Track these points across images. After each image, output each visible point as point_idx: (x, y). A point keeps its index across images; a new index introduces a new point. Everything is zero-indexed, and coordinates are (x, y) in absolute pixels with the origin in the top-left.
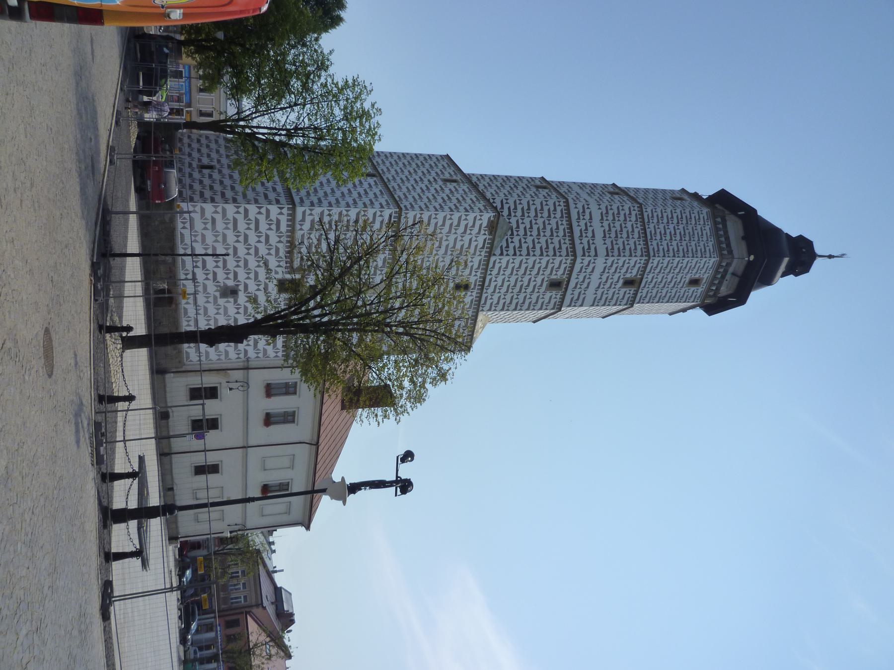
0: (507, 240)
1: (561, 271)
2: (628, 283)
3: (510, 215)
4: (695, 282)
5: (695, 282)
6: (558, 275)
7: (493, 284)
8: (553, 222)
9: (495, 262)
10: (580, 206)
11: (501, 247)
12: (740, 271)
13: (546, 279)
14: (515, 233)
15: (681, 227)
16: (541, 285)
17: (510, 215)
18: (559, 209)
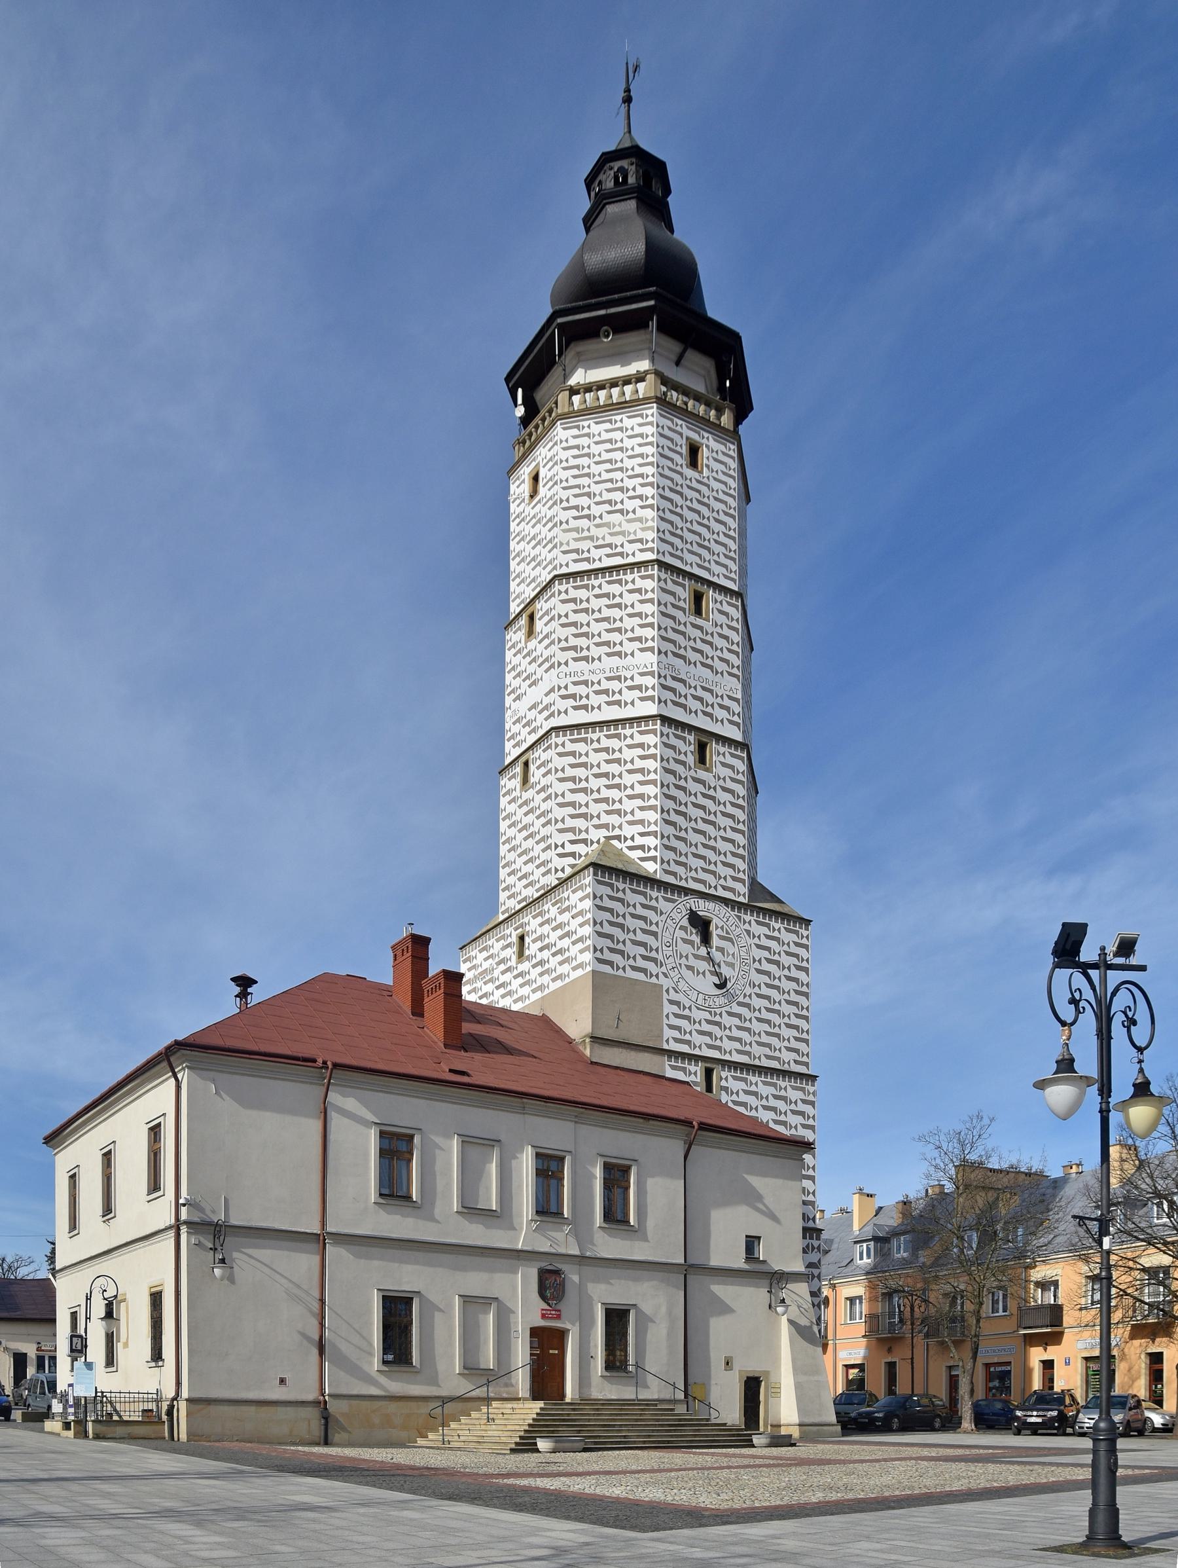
0: (630, 848)
1: (679, 744)
3: (585, 841)
6: (687, 747)
7: (702, 875)
8: (594, 758)
9: (666, 872)
10: (562, 704)
11: (642, 859)
12: (675, 347)
13: (692, 773)
14: (617, 832)
16: (703, 782)
17: (585, 841)
18: (570, 747)
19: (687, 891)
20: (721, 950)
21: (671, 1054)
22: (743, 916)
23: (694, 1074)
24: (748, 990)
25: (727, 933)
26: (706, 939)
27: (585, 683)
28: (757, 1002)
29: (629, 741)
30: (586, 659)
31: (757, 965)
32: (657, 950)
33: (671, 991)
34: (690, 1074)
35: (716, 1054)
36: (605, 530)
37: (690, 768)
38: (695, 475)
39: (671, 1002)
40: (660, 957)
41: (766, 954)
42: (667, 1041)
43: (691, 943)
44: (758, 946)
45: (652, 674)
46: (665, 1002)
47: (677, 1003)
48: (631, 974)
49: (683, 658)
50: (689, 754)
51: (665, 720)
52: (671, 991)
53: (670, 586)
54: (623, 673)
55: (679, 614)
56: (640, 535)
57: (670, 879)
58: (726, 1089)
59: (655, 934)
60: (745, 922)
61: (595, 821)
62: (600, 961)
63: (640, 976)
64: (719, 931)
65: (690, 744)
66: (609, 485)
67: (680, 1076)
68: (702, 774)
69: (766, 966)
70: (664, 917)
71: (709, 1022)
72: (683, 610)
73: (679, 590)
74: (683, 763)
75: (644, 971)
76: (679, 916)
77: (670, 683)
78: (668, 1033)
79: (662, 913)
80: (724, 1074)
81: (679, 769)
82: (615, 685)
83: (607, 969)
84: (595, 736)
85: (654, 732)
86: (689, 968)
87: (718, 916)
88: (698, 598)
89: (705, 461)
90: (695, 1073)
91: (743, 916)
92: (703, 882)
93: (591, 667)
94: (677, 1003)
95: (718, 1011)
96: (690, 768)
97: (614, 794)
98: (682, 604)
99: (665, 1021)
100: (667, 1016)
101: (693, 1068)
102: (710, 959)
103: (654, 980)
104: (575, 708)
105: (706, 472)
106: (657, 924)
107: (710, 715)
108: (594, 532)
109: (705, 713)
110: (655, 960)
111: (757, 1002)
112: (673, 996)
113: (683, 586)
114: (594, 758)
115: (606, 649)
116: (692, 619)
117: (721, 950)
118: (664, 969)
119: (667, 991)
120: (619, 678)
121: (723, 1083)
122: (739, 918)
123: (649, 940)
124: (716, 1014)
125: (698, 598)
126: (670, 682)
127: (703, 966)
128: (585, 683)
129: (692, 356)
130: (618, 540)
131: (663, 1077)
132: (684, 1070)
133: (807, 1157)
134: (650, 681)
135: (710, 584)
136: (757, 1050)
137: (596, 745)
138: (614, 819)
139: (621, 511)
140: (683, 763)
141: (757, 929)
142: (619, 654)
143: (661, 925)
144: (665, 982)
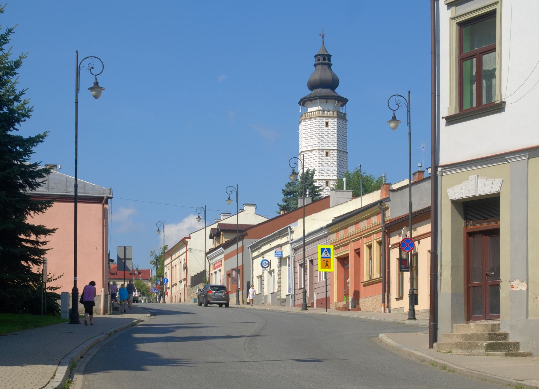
2: (327, 154)
4: (327, 124)
5: (327, 124)
55: (323, 158)
73: (323, 153)
88: (327, 153)
125: (327, 153)
129: (329, 101)
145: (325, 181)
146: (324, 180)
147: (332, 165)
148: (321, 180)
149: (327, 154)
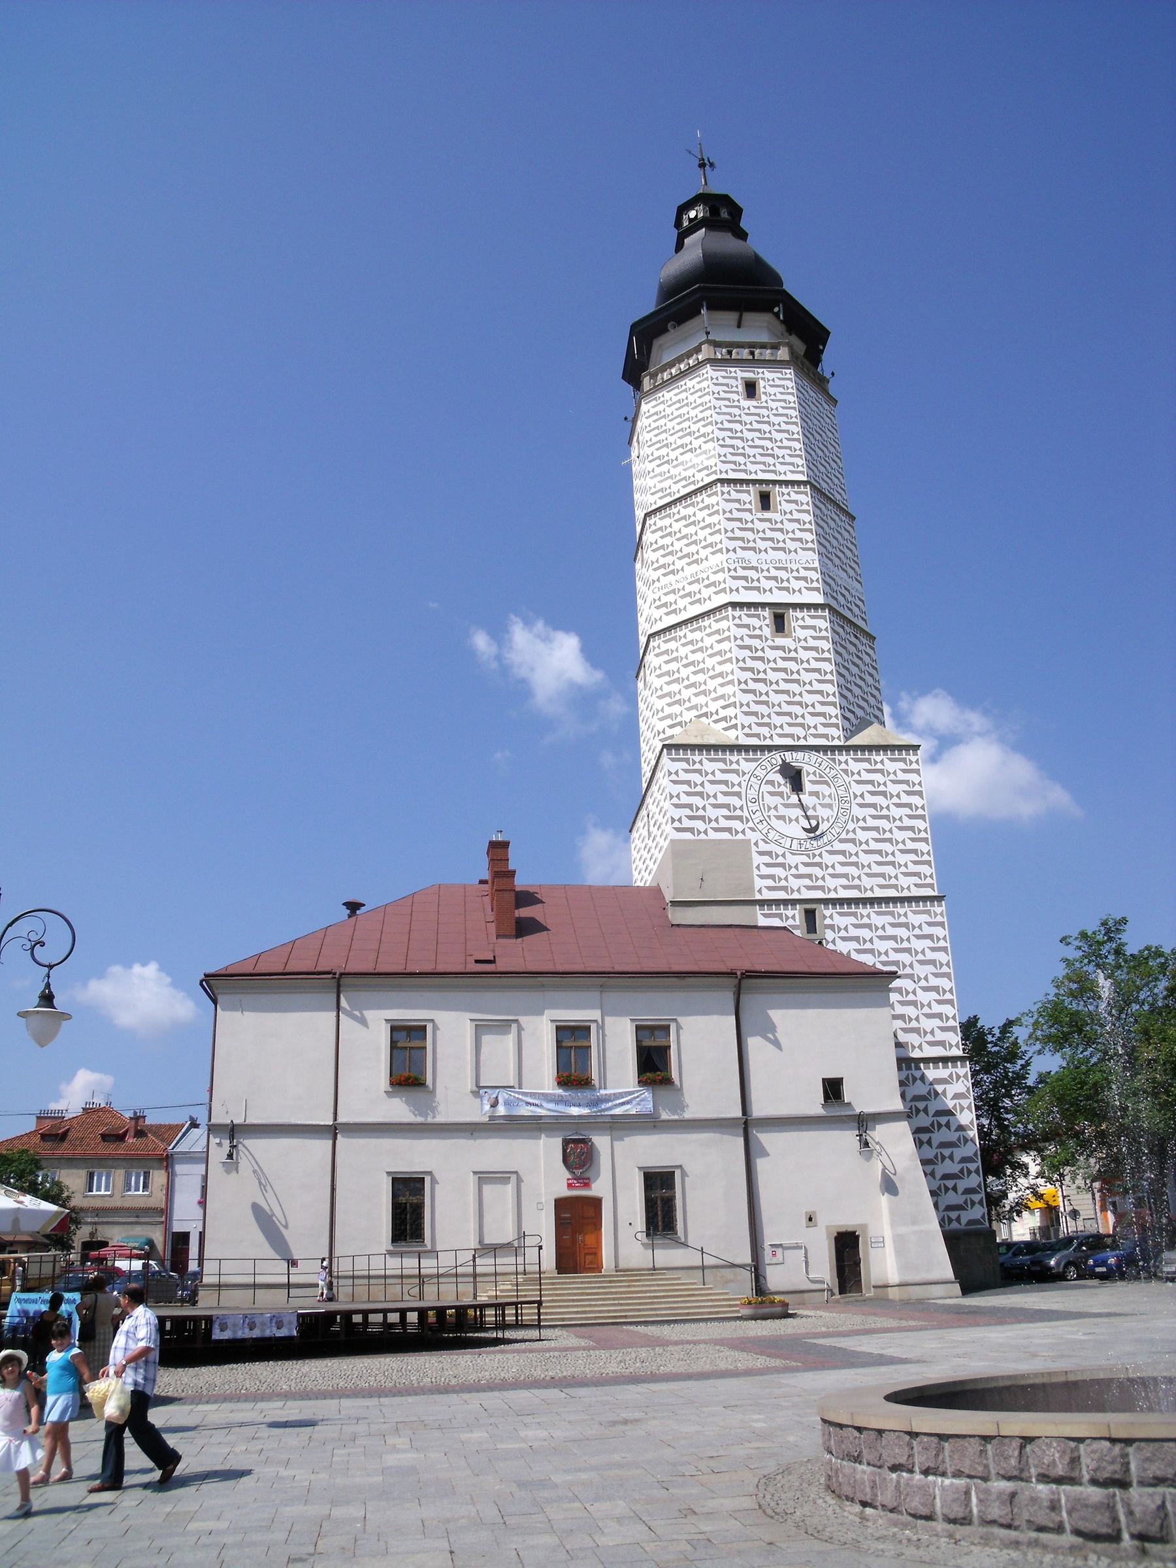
1: (755, 622)
2: (765, 501)
4: (751, 389)
5: (751, 389)
7: (788, 730)
9: (748, 735)
11: (725, 729)
12: (733, 316)
13: (770, 643)
14: (704, 710)
15: (671, 439)
16: (783, 648)
19: (770, 748)
20: (816, 794)
21: (762, 903)
22: (837, 757)
23: (794, 918)
24: (851, 826)
25: (821, 776)
26: (797, 786)
27: (673, 591)
28: (862, 836)
29: (708, 631)
30: (672, 572)
31: (859, 800)
32: (741, 808)
33: (761, 843)
34: (787, 918)
35: (819, 895)
36: (680, 468)
37: (767, 639)
38: (754, 403)
39: (761, 853)
40: (746, 814)
41: (870, 787)
42: (760, 891)
43: (781, 794)
44: (858, 782)
45: (722, 570)
46: (755, 855)
47: (769, 854)
48: (713, 835)
49: (754, 549)
50: (764, 627)
51: (734, 605)
52: (761, 843)
53: (734, 495)
54: (700, 576)
55: (747, 516)
56: (706, 463)
57: (754, 741)
58: (832, 927)
59: (738, 794)
60: (840, 763)
61: (687, 705)
62: (678, 830)
63: (725, 836)
64: (812, 777)
65: (765, 618)
66: (681, 434)
67: (776, 922)
68: (780, 641)
69: (869, 799)
70: (747, 777)
71: (806, 865)
72: (750, 511)
73: (744, 497)
74: (760, 637)
75: (729, 830)
76: (764, 772)
77: (741, 573)
78: (759, 883)
79: (744, 773)
80: (827, 913)
81: (756, 643)
82: (695, 587)
83: (687, 836)
84: (681, 634)
85: (726, 618)
86: (781, 818)
87: (806, 763)
89: (762, 390)
90: (793, 917)
91: (837, 757)
92: (792, 736)
93: (677, 577)
94: (769, 854)
95: (817, 852)
96: (767, 639)
97: (700, 678)
98: (748, 506)
99: (756, 872)
100: (758, 867)
101: (790, 913)
102: (801, 805)
103: (740, 836)
104: (667, 614)
105: (764, 398)
106: (739, 785)
107: (787, 589)
108: (673, 472)
109: (780, 589)
110: (740, 818)
111: (862, 836)
112: (763, 847)
113: (748, 492)
114: (683, 651)
115: (687, 560)
116: (759, 515)
117: (816, 794)
118: (751, 824)
119: (756, 844)
120: (697, 581)
121: (828, 921)
122: (834, 760)
123: (734, 801)
124: (814, 856)
126: (743, 574)
127: (798, 812)
128: (673, 591)
129: (748, 317)
130: (689, 473)
131: (756, 927)
132: (780, 916)
133: (896, 983)
134: (720, 577)
135: (774, 482)
136: (867, 882)
137: (683, 641)
138: (702, 700)
139: (691, 450)
140: (760, 637)
141: (854, 766)
142: (696, 561)
143: (744, 784)
144: (752, 836)
145: (767, 613)
146: (763, 605)
147: (791, 545)
148: (749, 605)
149: (765, 501)
